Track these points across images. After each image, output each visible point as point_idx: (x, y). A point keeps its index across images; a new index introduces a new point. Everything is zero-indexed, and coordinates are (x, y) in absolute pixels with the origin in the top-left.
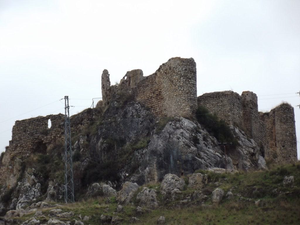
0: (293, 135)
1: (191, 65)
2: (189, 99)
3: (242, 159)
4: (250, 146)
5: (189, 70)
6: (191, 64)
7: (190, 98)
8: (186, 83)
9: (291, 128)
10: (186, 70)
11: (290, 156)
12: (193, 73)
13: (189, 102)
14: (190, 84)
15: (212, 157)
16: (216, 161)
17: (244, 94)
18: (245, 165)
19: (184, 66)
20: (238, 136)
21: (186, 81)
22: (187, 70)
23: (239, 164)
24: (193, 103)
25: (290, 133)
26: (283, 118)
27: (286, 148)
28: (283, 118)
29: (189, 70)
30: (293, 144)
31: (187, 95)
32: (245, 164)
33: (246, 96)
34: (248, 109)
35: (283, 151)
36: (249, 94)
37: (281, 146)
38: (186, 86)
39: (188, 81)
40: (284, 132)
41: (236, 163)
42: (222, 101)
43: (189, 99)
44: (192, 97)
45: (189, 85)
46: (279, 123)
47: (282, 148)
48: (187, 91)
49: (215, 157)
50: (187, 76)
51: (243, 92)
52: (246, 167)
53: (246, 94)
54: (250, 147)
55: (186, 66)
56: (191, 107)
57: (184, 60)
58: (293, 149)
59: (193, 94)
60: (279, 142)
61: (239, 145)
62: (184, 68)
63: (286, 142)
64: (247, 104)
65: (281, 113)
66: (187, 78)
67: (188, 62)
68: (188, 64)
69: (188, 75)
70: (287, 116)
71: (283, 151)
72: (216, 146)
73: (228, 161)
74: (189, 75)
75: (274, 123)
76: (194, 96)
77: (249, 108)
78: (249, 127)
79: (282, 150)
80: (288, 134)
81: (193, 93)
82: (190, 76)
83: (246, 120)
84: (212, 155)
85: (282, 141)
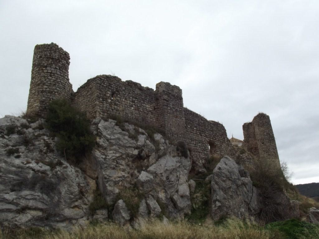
0: (270, 134)
1: (50, 51)
2: (40, 92)
3: (101, 168)
4: (128, 145)
5: (44, 56)
6: (49, 50)
7: (41, 90)
8: (38, 73)
9: (267, 129)
10: (40, 57)
11: (269, 150)
12: (51, 60)
13: (39, 96)
14: (44, 73)
15: (10, 172)
16: (18, 180)
17: (157, 86)
18: (106, 178)
19: (39, 53)
20: (100, 132)
21: (39, 70)
22: (42, 57)
23: (99, 177)
24: (46, 96)
25: (267, 133)
26: (260, 123)
27: (265, 145)
28: (260, 123)
29: (44, 56)
30: (270, 141)
31: (37, 87)
32: (106, 176)
33: (159, 87)
34: (161, 102)
35: (263, 147)
36: (161, 85)
37: (261, 143)
38: (39, 76)
39: (42, 69)
40: (262, 133)
41: (96, 176)
42: (91, 88)
43: (40, 92)
44: (46, 88)
45: (42, 74)
46: (257, 127)
47: (262, 145)
48: (39, 82)
49: (21, 171)
50: (41, 64)
51: (157, 85)
52: (107, 182)
53: (159, 85)
54: (130, 147)
55: (41, 53)
56: (42, 102)
57: (40, 47)
58: (271, 144)
59: (47, 85)
60: (259, 140)
61: (99, 146)
62: (39, 56)
63: (264, 140)
64: (160, 96)
65: (258, 120)
66: (41, 67)
67: (45, 48)
68: (45, 49)
69: (41, 63)
70: (263, 122)
71: (263, 147)
72: (52, 151)
73: (63, 175)
74: (44, 62)
75: (254, 128)
76: (50, 87)
77: (162, 101)
78: (163, 123)
79: (262, 146)
80: (265, 134)
81: (47, 84)
82: (46, 63)
83: (159, 115)
84: (14, 169)
85: (261, 139)
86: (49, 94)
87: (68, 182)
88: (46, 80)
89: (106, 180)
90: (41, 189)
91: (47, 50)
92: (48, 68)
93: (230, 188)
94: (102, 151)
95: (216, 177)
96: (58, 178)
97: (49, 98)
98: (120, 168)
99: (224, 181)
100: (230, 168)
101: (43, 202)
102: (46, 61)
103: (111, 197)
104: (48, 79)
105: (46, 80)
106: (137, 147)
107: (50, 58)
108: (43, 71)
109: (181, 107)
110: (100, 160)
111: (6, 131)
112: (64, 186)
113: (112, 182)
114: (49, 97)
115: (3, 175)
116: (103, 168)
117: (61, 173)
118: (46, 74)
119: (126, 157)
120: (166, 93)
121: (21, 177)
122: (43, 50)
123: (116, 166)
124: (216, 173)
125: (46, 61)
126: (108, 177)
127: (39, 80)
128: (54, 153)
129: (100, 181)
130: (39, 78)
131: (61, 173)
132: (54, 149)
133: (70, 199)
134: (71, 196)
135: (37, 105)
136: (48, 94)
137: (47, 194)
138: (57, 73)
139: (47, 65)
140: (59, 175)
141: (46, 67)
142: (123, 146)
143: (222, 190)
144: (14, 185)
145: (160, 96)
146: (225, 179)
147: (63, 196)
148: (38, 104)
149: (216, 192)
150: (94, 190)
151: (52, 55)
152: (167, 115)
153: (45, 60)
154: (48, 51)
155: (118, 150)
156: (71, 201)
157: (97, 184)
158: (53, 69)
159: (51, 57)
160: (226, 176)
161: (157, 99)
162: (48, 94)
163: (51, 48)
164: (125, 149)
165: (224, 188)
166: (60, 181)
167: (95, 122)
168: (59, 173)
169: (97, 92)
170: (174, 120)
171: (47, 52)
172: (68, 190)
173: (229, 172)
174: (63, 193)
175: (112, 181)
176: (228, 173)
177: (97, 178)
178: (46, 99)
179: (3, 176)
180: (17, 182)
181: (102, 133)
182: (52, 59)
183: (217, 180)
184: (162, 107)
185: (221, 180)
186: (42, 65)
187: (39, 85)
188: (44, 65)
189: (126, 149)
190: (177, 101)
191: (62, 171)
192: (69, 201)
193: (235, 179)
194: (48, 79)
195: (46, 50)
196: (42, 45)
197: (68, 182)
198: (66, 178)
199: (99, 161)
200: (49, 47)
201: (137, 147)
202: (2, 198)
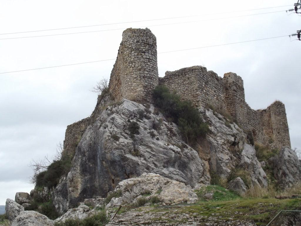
0: (285, 124)
1: (146, 36)
2: (142, 77)
3: (216, 152)
4: (228, 133)
5: (142, 42)
6: (145, 35)
7: (143, 75)
8: (137, 58)
9: (283, 119)
10: (138, 42)
11: (284, 140)
12: (148, 46)
13: (141, 81)
14: (143, 58)
15: (160, 152)
16: (167, 159)
17: (226, 76)
18: (220, 160)
19: (135, 38)
20: (210, 120)
21: (138, 55)
22: (139, 42)
23: (212, 159)
24: (148, 82)
25: (283, 123)
26: (277, 112)
27: (281, 134)
28: (277, 112)
29: (142, 42)
30: (286, 131)
31: (139, 72)
32: (220, 158)
33: (229, 77)
34: (231, 92)
35: (278, 136)
36: (231, 76)
37: (277, 133)
38: (138, 61)
39: (141, 55)
40: (278, 122)
41: (208, 158)
42: (188, 78)
43: (142, 77)
44: (147, 74)
45: (142, 59)
46: (274, 116)
47: (278, 134)
48: (140, 67)
49: (167, 152)
50: (140, 49)
51: (225, 75)
52: (222, 163)
53: (228, 75)
54: (229, 134)
55: (138, 38)
56: (145, 87)
57: (136, 31)
58: (286, 134)
59: (147, 71)
60: (274, 130)
61: (211, 132)
62: (136, 40)
63: (280, 129)
64: (229, 86)
65: (275, 108)
66: (139, 52)
67: (141, 33)
68: (141, 34)
69: (140, 48)
70: (279, 110)
71: (278, 136)
72: (175, 135)
73: (192, 156)
74: (142, 47)
75: (270, 117)
76: (150, 73)
77: (232, 91)
78: (233, 112)
79: (277, 136)
80: (281, 123)
81: (147, 70)
82: (144, 48)
83: (229, 105)
84: (161, 149)
85: (277, 129)
86: (150, 80)
87: (196, 161)
88: (146, 65)
89: (220, 162)
90: (179, 166)
91: (144, 36)
92: (147, 54)
93: (296, 173)
94: (214, 137)
95: (288, 164)
96: (188, 158)
97: (150, 83)
98: (226, 152)
99: (292, 167)
100: (294, 156)
101: (182, 177)
102: (143, 46)
103: (225, 175)
104: (147, 64)
105: (146, 65)
106: (234, 135)
107: (147, 43)
108: (142, 56)
109: (243, 97)
110: (215, 144)
111: (138, 115)
112: (193, 165)
113: (224, 163)
114: (150, 82)
115: (156, 154)
116: (217, 151)
117: (190, 154)
118: (145, 59)
119: (227, 143)
120: (235, 83)
121: (168, 156)
122: (140, 35)
123: (223, 150)
124: (288, 160)
125: (143, 46)
126: (222, 159)
127: (140, 65)
128: (177, 137)
129: (214, 163)
130: (140, 63)
131: (190, 154)
132: (176, 133)
133: (199, 175)
134: (199, 173)
135: (141, 90)
136: (149, 80)
137: (182, 171)
138: (153, 59)
139: (145, 50)
140: (189, 156)
141: (144, 53)
142: (224, 134)
143: (292, 174)
144: (164, 163)
145: (229, 86)
146: (293, 165)
147: (193, 173)
148: (142, 88)
149: (288, 176)
150: (209, 169)
151: (148, 41)
152: (237, 105)
153: (143, 45)
154: (145, 36)
155: (222, 137)
156: (199, 177)
157: (210, 164)
158: (150, 55)
159: (148, 43)
160: (294, 163)
161: (227, 89)
162: (149, 80)
163: (147, 33)
164: (226, 136)
165: (293, 172)
166: (190, 160)
167: (201, 112)
168: (188, 154)
169: (198, 83)
170: (241, 110)
171: (143, 37)
172: (196, 169)
173: (295, 160)
174: (193, 171)
175: (224, 162)
176: (295, 161)
177: (210, 159)
178: (148, 84)
179: (156, 155)
180: (167, 160)
181: (212, 121)
182: (148, 44)
183: (288, 166)
184: (232, 97)
185: (291, 166)
186: (140, 50)
187: (140, 70)
188: (142, 50)
189: (227, 136)
190: (241, 92)
191: (190, 153)
192: (198, 177)
193: (299, 166)
194: (147, 64)
195: (143, 35)
196: (137, 30)
197: (196, 161)
198: (194, 159)
199: (214, 145)
200: (145, 33)
201: (234, 135)
202: (162, 173)
